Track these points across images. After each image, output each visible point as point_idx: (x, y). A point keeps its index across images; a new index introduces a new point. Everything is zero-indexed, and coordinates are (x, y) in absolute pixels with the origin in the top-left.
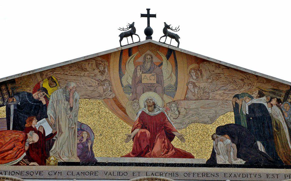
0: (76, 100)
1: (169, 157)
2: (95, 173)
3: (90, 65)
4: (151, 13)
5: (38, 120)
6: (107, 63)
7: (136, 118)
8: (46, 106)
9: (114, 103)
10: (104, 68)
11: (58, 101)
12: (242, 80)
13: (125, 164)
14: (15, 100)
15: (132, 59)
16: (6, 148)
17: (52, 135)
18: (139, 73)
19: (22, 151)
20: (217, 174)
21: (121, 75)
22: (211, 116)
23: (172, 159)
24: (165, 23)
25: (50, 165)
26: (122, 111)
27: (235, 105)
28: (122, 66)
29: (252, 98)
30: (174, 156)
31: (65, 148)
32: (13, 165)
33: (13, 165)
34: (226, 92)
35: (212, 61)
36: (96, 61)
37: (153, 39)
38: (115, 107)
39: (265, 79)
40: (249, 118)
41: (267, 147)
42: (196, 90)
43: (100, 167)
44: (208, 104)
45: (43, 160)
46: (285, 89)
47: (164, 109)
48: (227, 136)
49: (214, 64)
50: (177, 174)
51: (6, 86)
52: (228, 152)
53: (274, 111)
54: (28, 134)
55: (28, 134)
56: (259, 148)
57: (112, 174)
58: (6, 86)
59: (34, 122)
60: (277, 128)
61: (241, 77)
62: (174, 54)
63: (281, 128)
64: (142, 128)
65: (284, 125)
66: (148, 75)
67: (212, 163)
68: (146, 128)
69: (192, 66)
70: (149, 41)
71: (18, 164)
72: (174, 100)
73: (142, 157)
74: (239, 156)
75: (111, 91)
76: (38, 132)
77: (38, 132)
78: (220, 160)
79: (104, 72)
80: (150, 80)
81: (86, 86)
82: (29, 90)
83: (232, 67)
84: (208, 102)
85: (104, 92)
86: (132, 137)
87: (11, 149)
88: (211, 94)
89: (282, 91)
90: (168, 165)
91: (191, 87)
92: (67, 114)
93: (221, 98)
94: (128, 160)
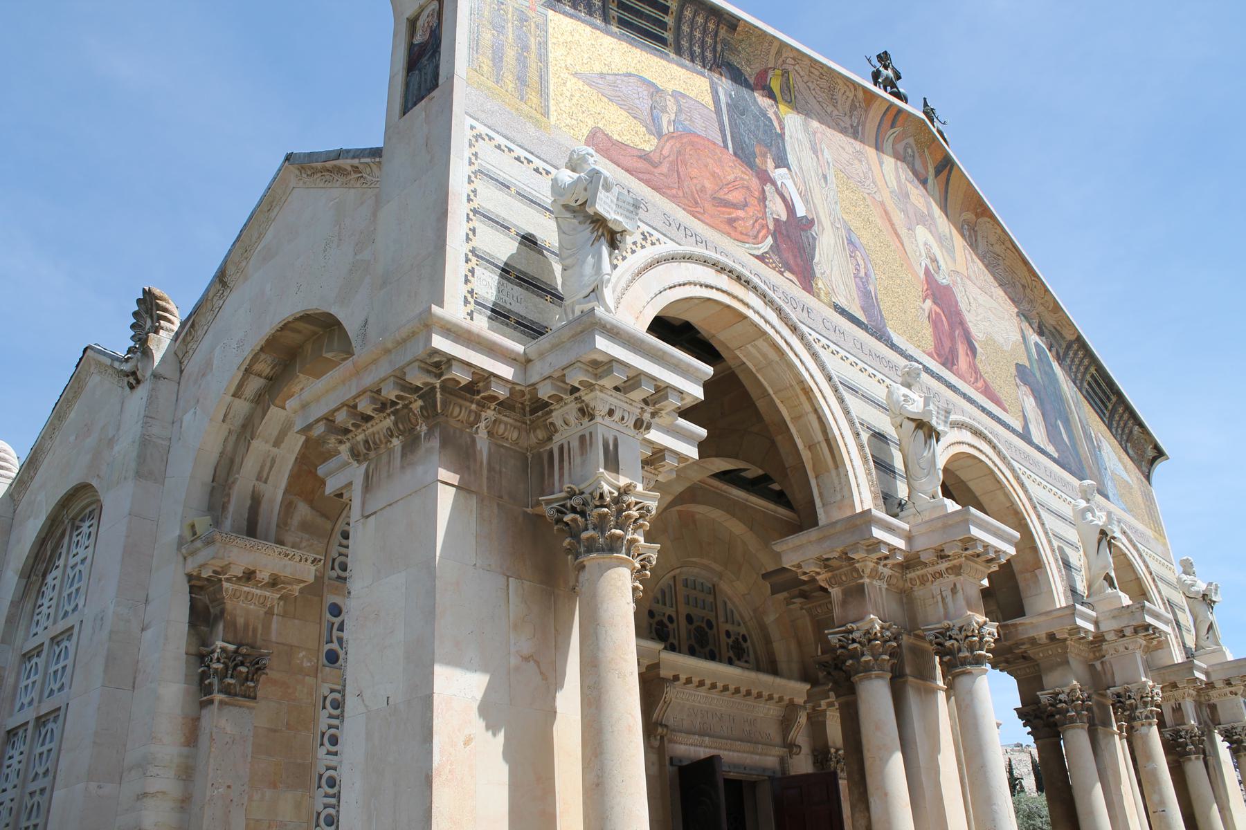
8: (782, 135)
12: (1023, 286)
15: (892, 137)
24: (925, 99)
25: (821, 301)
32: (753, 255)
33: (753, 255)
36: (855, 95)
41: (1069, 437)
44: (995, 309)
49: (999, 231)
58: (718, 26)
61: (1024, 281)
62: (950, 172)
79: (858, 133)
90: (983, 410)
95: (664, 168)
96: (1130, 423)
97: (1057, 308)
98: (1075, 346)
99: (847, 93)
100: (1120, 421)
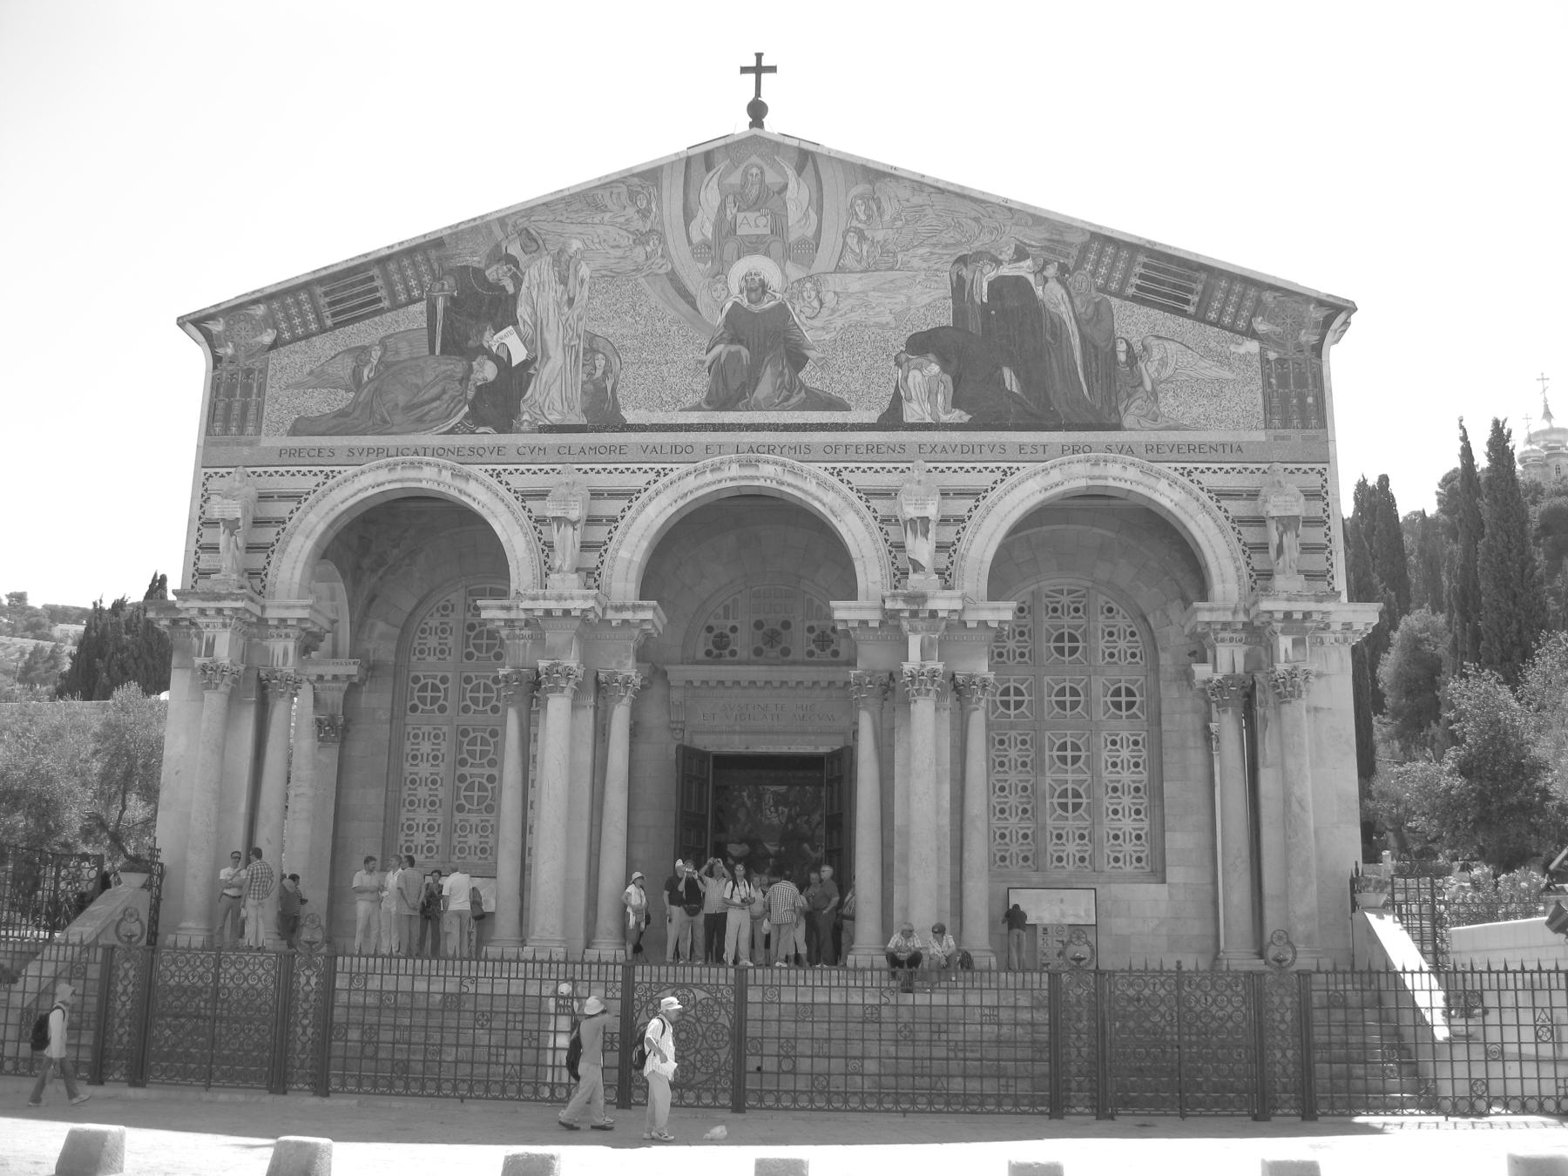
0: (582, 281)
1: (794, 409)
2: (621, 449)
3: (614, 196)
4: (765, 63)
5: (498, 329)
6: (654, 191)
7: (720, 319)
8: (515, 297)
9: (669, 283)
10: (649, 203)
11: (541, 285)
12: (976, 220)
13: (688, 428)
14: (446, 287)
15: (715, 179)
16: (427, 397)
17: (525, 364)
18: (731, 211)
19: (460, 401)
20: (902, 447)
21: (688, 215)
22: (898, 308)
23: (797, 413)
26: (688, 302)
27: (958, 282)
28: (692, 197)
29: (999, 263)
30: (802, 407)
31: (555, 394)
34: (937, 250)
35: (904, 175)
37: (767, 127)
38: (672, 293)
39: (1033, 216)
40: (989, 312)
41: (1025, 381)
42: (865, 248)
43: (632, 434)
44: (892, 282)
45: (506, 421)
46: (1078, 239)
47: (786, 296)
48: (931, 356)
49: (907, 183)
50: (808, 447)
51: (425, 252)
52: (931, 395)
53: (1051, 294)
54: (474, 363)
55: (474, 363)
56: (1007, 384)
57: (658, 450)
58: (425, 252)
59: (487, 335)
60: (1054, 335)
61: (973, 214)
63: (1064, 336)
64: (731, 342)
65: (1072, 327)
66: (751, 216)
67: (892, 419)
68: (740, 342)
69: (855, 191)
70: (756, 131)
71: (451, 432)
72: (811, 273)
73: (729, 410)
74: (956, 403)
75: (662, 256)
76: (496, 358)
77: (496, 358)
78: (913, 412)
79: (650, 211)
80: (757, 226)
81: (607, 247)
82: (475, 261)
83: (951, 188)
84: (890, 275)
85: (647, 258)
86: (707, 364)
87: (438, 398)
88: (899, 257)
89: (1070, 245)
90: (787, 428)
91: (852, 240)
92: (560, 314)
93: (925, 265)
94: (695, 418)
95: (357, 413)
96: (1252, 293)
97: (1037, 219)
98: (1095, 246)
99: (615, 191)
100: (1227, 297)
